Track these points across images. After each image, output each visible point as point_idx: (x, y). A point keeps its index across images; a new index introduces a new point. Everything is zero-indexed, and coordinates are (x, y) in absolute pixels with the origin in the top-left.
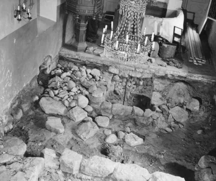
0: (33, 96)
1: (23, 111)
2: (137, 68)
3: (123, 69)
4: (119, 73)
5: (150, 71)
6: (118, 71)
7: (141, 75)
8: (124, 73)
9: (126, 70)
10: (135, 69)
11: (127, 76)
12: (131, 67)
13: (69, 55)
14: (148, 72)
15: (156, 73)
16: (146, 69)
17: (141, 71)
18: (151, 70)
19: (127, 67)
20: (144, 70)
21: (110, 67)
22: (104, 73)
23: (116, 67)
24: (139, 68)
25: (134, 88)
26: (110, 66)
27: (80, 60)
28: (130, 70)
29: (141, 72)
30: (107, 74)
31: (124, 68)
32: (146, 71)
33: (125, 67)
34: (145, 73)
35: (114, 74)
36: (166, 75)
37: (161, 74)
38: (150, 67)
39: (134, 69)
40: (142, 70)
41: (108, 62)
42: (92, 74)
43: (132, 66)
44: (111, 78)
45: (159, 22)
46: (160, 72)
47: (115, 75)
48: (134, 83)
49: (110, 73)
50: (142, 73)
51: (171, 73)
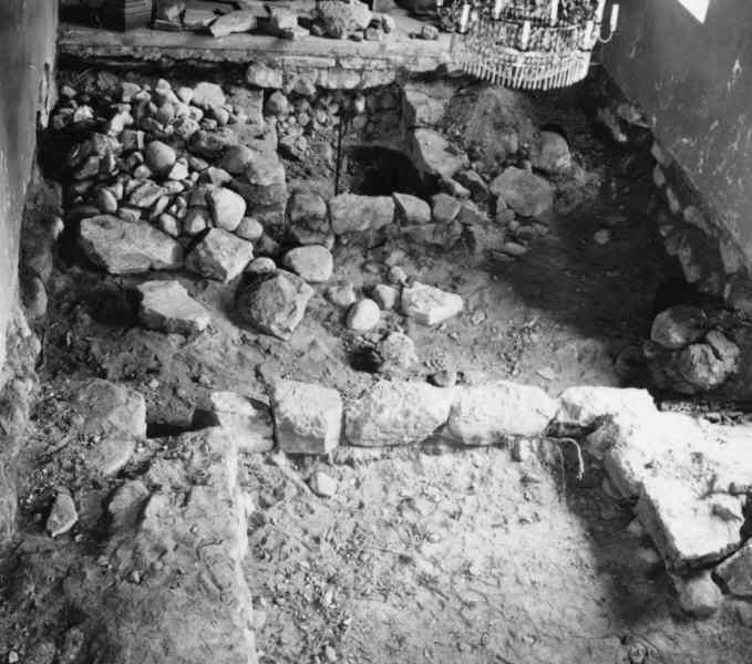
0: (47, 223)
1: (42, 280)
2: (344, 58)
3: (298, 67)
4: (285, 83)
5: (388, 61)
6: (281, 78)
7: (359, 78)
8: (301, 82)
9: (308, 69)
10: (337, 62)
11: (312, 90)
12: (322, 56)
13: (95, 46)
14: (382, 65)
15: (407, 66)
16: (373, 58)
17: (358, 67)
18: (392, 57)
19: (311, 60)
21: (252, 68)
23: (271, 65)
24: (349, 57)
26: (251, 63)
27: (141, 59)
28: (320, 68)
31: (300, 64)
32: (374, 63)
35: (265, 89)
36: (442, 67)
37: (426, 65)
38: (388, 48)
39: (333, 63)
40: (362, 62)
41: (242, 50)
42: (198, 101)
44: (260, 103)
46: (421, 61)
47: (269, 92)
49: (254, 88)
50: (361, 72)
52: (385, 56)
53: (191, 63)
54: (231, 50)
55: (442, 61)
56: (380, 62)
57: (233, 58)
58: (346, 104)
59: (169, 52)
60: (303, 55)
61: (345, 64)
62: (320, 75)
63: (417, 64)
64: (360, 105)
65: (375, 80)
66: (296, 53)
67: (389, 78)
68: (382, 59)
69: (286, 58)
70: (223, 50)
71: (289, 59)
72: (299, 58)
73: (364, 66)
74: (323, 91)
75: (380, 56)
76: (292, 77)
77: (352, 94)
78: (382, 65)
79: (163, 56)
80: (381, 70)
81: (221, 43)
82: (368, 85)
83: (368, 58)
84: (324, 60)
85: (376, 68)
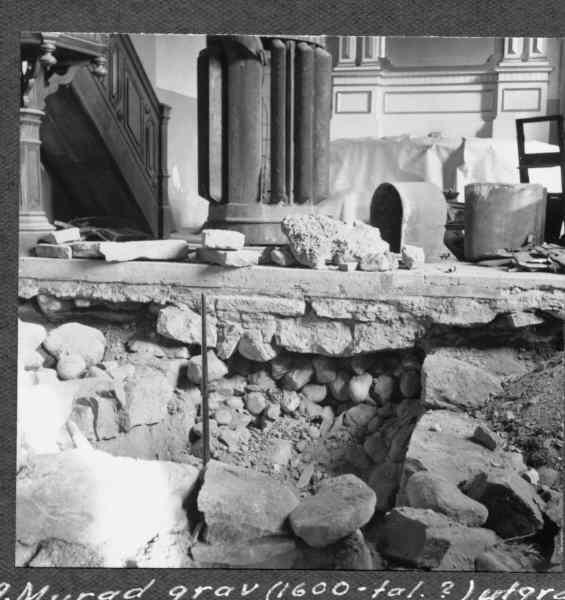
3: (241, 313)
5: (399, 307)
7: (350, 338)
8: (246, 337)
10: (309, 307)
11: (268, 354)
12: (283, 296)
14: (389, 313)
15: (435, 315)
16: (370, 301)
18: (405, 300)
20: (362, 306)
21: (165, 312)
22: (136, 346)
24: (328, 298)
25: (318, 421)
29: (345, 322)
30: (147, 350)
31: (244, 308)
32: (372, 309)
33: (244, 302)
34: (368, 323)
36: (503, 318)
37: (470, 314)
39: (301, 308)
40: (352, 308)
42: (51, 346)
43: (284, 291)
44: (174, 367)
45: (445, 155)
48: (320, 393)
50: (351, 323)
51: (535, 304)
52: (392, 298)
53: (79, 304)
54: (139, 284)
55: (502, 307)
56: (385, 308)
57: (140, 296)
58: (338, 386)
59: (49, 286)
60: (250, 294)
61: (321, 310)
62: (279, 329)
63: (454, 313)
64: (361, 387)
65: (377, 340)
66: (238, 291)
67: (401, 337)
68: (386, 302)
69: (221, 297)
70: (124, 283)
71: (225, 299)
72: (244, 298)
73: (354, 314)
74: (290, 358)
75: (382, 298)
76: (231, 328)
77: (344, 365)
78: (389, 313)
79: (41, 292)
80: (389, 323)
81: (121, 273)
82: (363, 347)
83: (361, 300)
84: (284, 301)
85: (378, 319)
